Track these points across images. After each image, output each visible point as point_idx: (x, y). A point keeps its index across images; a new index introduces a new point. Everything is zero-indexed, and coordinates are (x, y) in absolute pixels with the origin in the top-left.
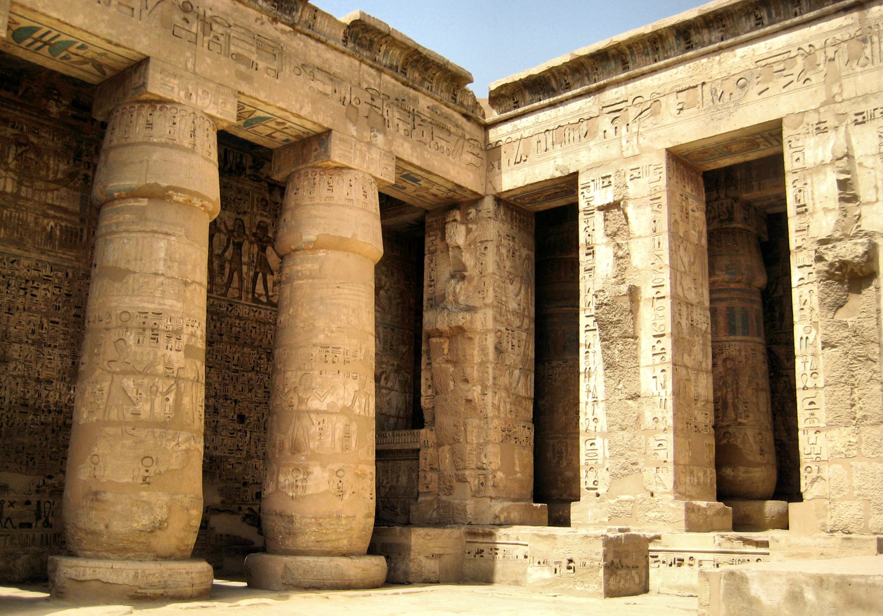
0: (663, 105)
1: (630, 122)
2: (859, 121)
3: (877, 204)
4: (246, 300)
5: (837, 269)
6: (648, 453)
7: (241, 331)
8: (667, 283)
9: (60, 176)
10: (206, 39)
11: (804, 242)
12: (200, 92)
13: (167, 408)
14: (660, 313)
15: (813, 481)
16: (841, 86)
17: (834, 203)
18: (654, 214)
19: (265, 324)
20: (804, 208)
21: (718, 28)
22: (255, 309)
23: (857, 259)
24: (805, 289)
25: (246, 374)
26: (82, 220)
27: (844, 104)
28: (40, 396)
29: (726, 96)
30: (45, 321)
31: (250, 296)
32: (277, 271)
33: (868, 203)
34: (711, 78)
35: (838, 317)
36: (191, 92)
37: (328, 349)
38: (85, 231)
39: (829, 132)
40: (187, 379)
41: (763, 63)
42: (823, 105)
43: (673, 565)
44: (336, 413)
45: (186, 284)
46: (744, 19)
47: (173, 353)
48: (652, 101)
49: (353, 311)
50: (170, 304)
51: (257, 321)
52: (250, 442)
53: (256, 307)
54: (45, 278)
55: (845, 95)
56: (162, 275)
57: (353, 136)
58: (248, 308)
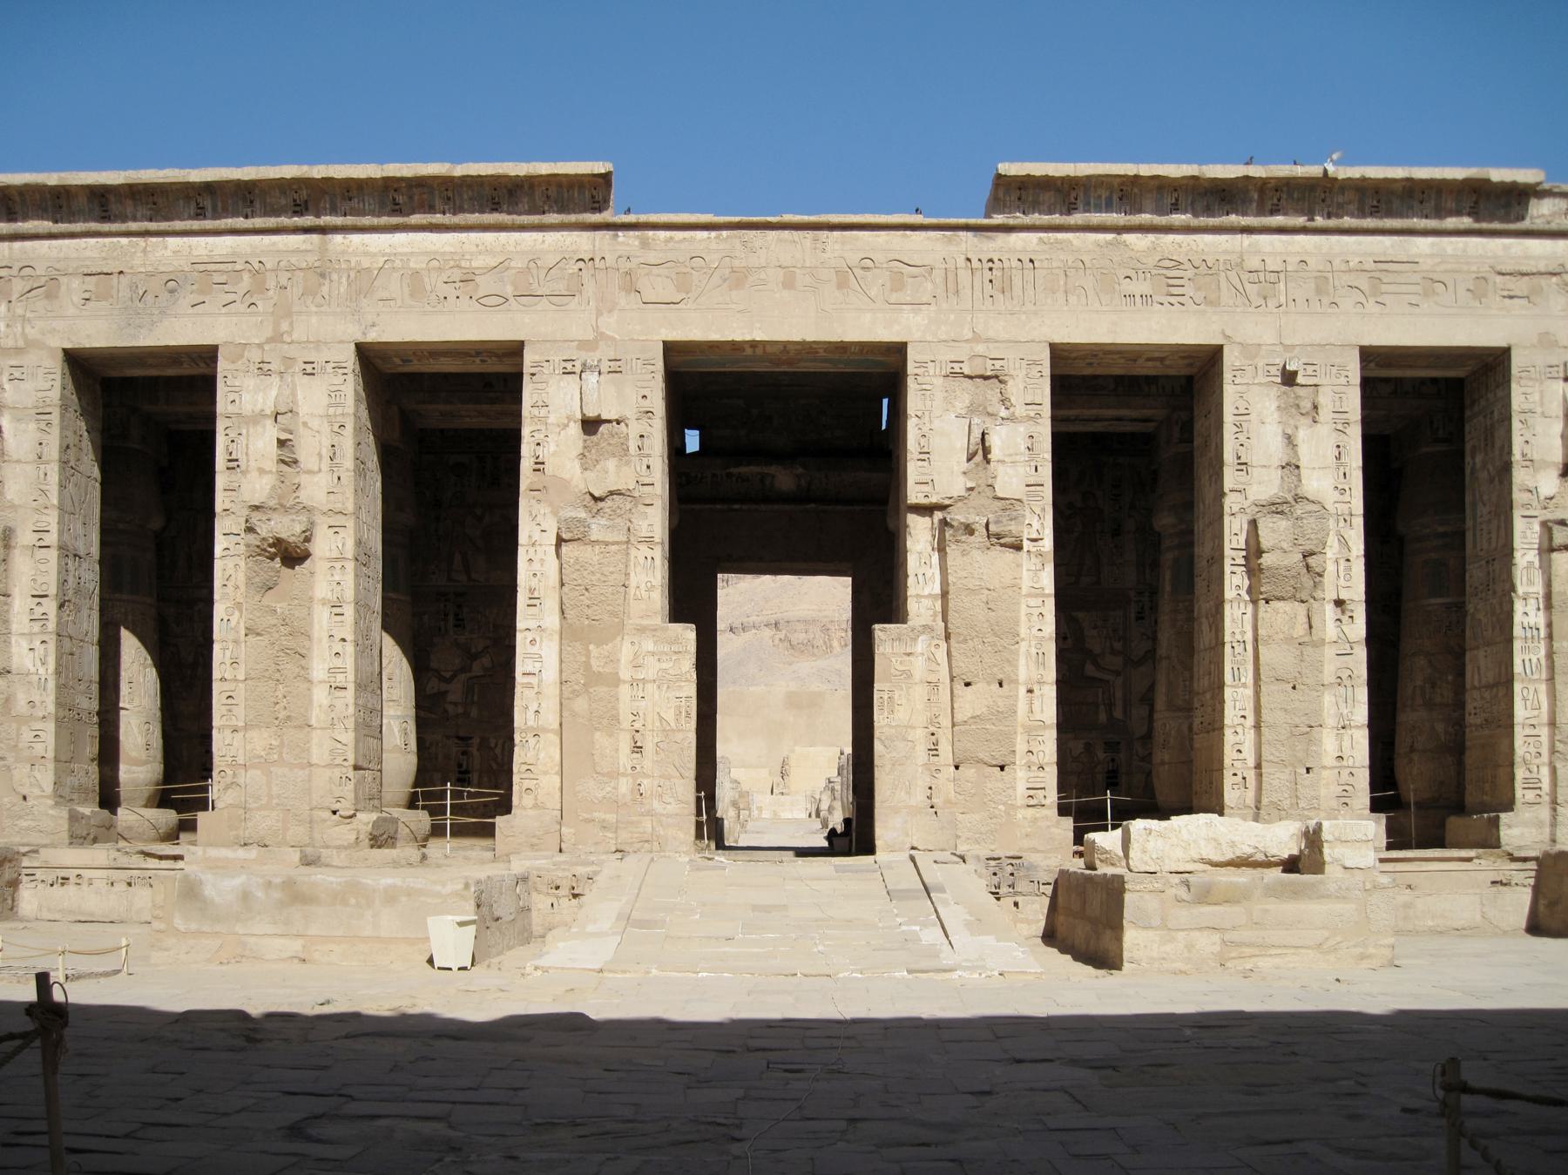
0: (63, 288)
1: (14, 298)
2: (309, 370)
3: (320, 475)
5: (270, 546)
6: (20, 745)
8: (54, 528)
11: (233, 504)
14: (43, 568)
15: (227, 788)
16: (291, 324)
17: (271, 465)
18: (39, 435)
20: (236, 463)
21: (147, 204)
23: (294, 538)
24: (230, 563)
27: (292, 346)
29: (149, 298)
33: (310, 472)
34: (132, 268)
35: (265, 601)
39: (273, 376)
41: (202, 267)
42: (270, 340)
43: (55, 886)
46: (181, 202)
48: (47, 278)
55: (295, 336)
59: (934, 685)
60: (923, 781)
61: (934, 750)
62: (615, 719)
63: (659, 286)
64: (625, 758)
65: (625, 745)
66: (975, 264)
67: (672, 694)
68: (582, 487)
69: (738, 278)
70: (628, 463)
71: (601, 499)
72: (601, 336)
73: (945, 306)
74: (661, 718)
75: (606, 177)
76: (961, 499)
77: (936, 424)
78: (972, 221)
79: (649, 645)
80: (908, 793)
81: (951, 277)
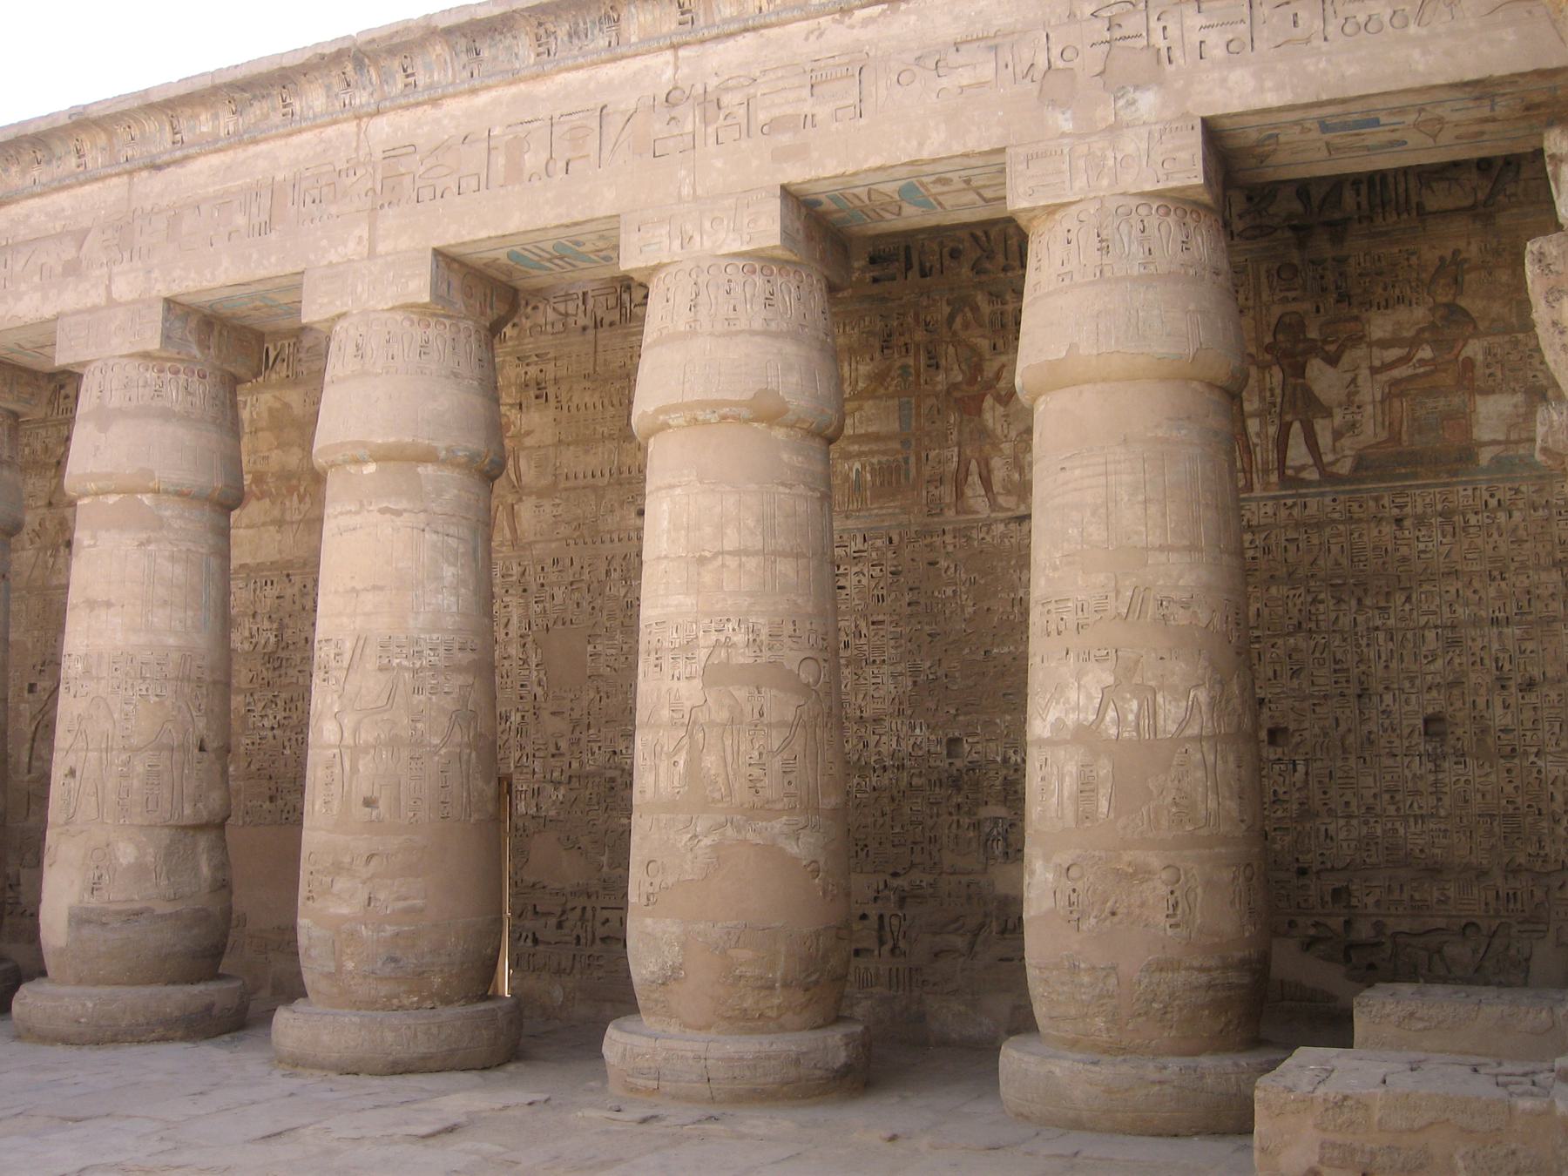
4: (1265, 490)
7: (1258, 555)
9: (861, 385)
10: (711, 130)
12: (707, 225)
13: (677, 778)
19: (1319, 526)
22: (1289, 502)
25: (1280, 642)
26: (905, 443)
28: (866, 745)
30: (862, 624)
31: (1274, 478)
32: (1340, 405)
36: (691, 233)
37: (1049, 607)
38: (912, 460)
40: (712, 723)
44: (1066, 742)
45: (702, 561)
47: (683, 684)
49: (1094, 514)
50: (676, 602)
51: (1297, 525)
52: (1306, 782)
53: (1291, 496)
54: (856, 555)
56: (666, 557)
57: (1063, 135)
58: (1270, 503)
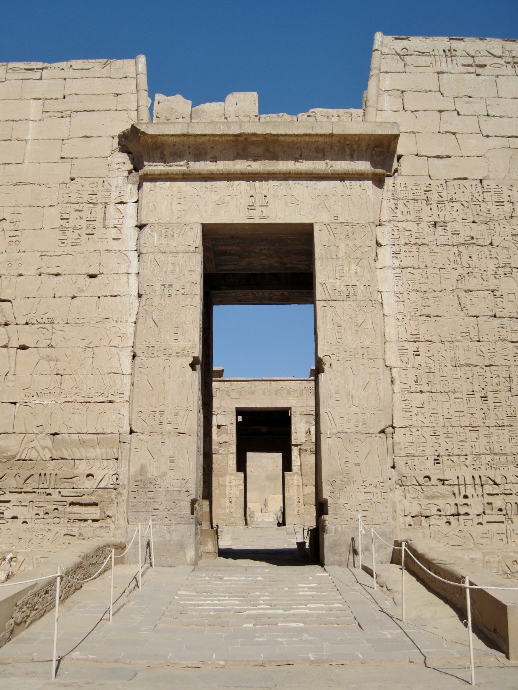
59: (299, 486)
60: (296, 509)
61: (299, 501)
62: (225, 495)
63: (234, 395)
64: (227, 504)
65: (227, 501)
66: (307, 388)
67: (238, 489)
68: (217, 441)
69: (252, 392)
70: (228, 435)
71: (221, 444)
72: (221, 406)
73: (300, 398)
74: (236, 495)
75: (222, 371)
76: (304, 443)
77: (298, 426)
78: (306, 379)
79: (233, 478)
80: (293, 511)
81: (301, 392)
